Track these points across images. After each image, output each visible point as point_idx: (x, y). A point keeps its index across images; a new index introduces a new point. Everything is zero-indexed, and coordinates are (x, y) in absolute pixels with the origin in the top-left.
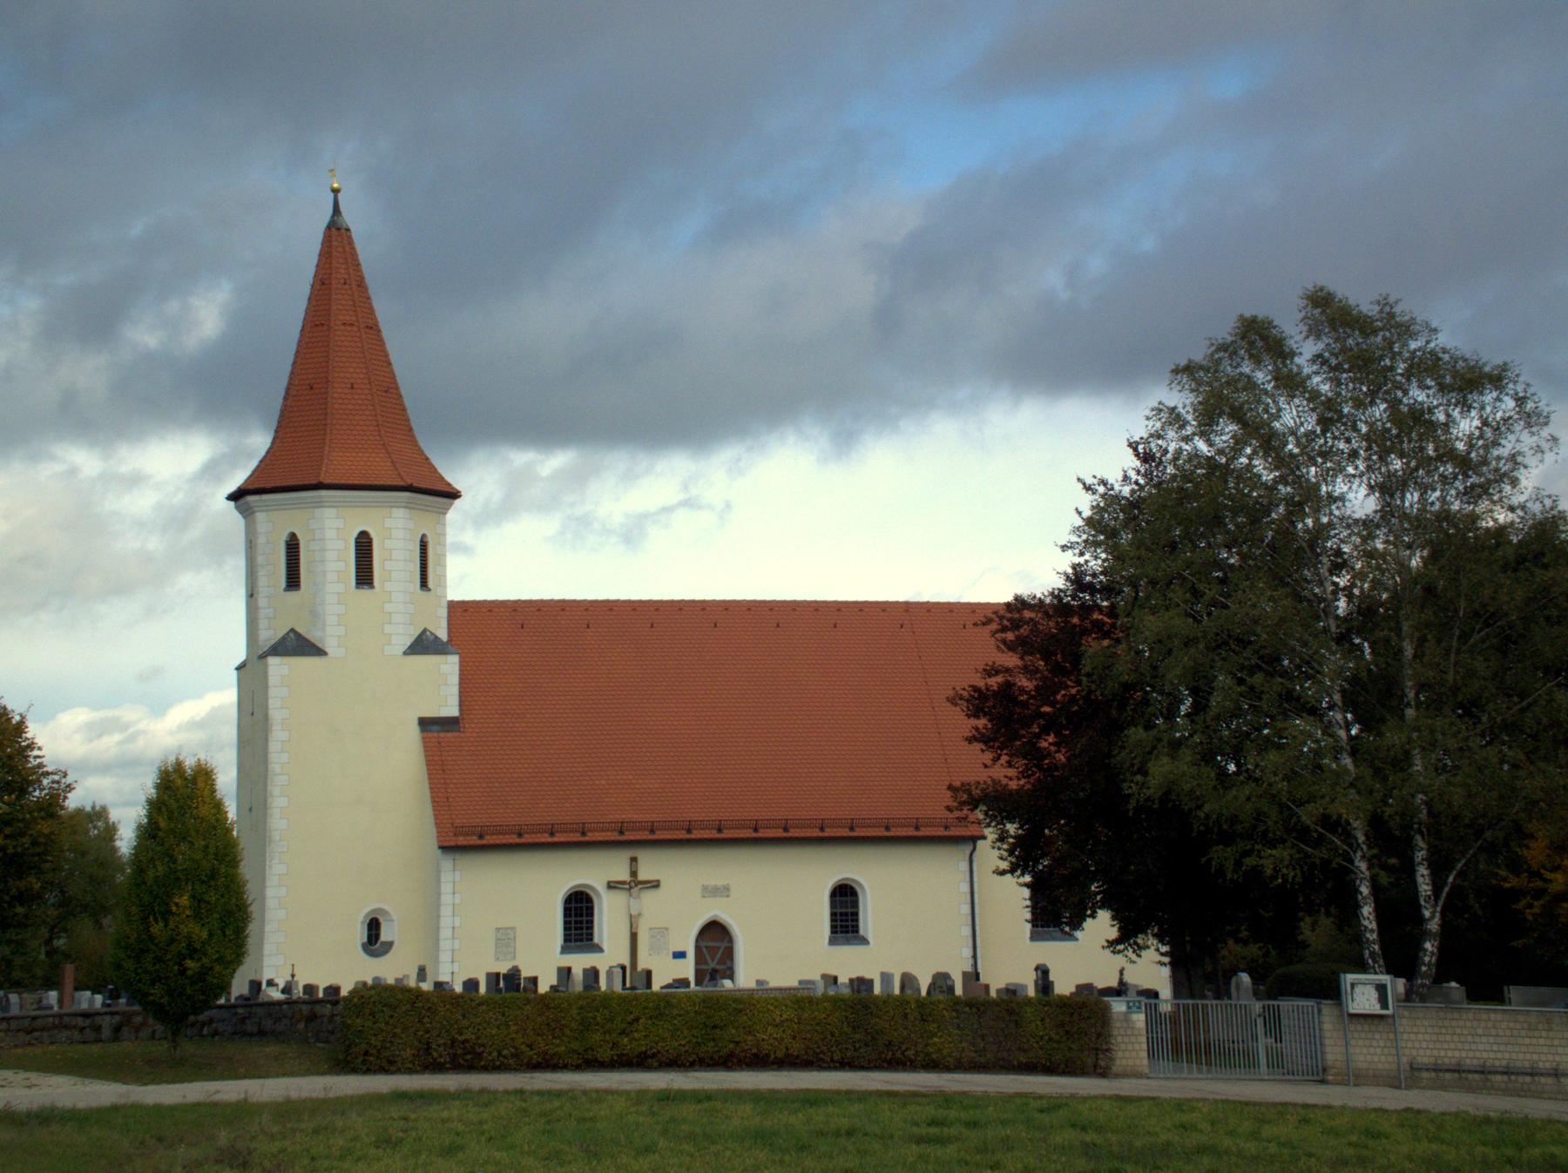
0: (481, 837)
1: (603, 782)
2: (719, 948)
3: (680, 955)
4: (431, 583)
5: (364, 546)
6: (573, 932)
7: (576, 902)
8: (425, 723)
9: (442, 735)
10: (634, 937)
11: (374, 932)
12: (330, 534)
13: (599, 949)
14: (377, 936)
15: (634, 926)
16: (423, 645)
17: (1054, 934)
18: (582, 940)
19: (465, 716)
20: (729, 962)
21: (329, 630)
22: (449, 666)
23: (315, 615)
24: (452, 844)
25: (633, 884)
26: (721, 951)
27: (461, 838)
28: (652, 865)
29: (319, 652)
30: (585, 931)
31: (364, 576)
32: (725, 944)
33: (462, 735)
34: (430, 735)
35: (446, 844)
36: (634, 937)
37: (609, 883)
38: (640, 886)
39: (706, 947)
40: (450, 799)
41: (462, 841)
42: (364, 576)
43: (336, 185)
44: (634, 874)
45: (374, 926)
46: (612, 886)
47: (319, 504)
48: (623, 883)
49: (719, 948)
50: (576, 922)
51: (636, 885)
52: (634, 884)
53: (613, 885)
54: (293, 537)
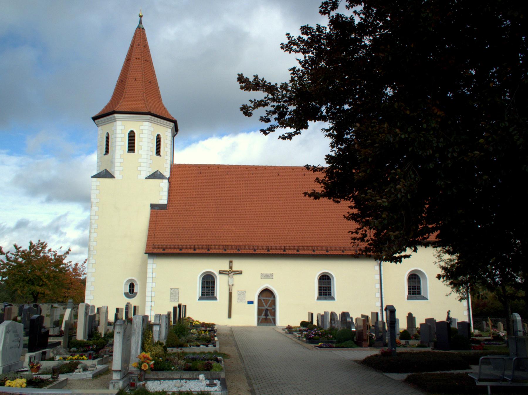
2: (269, 300)
3: (251, 302)
4: (162, 154)
5: (132, 136)
8: (153, 206)
9: (159, 211)
10: (230, 294)
11: (132, 288)
12: (118, 131)
14: (133, 290)
15: (230, 290)
16: (156, 176)
17: (418, 297)
19: (170, 204)
21: (116, 169)
22: (164, 184)
23: (112, 163)
25: (230, 272)
26: (270, 301)
27: (155, 250)
28: (238, 264)
29: (112, 177)
30: (210, 291)
31: (131, 148)
32: (272, 299)
33: (167, 211)
34: (154, 210)
36: (230, 294)
37: (220, 271)
39: (264, 300)
40: (156, 235)
41: (155, 251)
42: (131, 148)
43: (141, 14)
44: (231, 268)
45: (132, 286)
46: (221, 273)
47: (115, 120)
48: (226, 271)
49: (269, 300)
50: (207, 287)
51: (232, 273)
52: (231, 272)
53: (221, 272)
54: (108, 133)
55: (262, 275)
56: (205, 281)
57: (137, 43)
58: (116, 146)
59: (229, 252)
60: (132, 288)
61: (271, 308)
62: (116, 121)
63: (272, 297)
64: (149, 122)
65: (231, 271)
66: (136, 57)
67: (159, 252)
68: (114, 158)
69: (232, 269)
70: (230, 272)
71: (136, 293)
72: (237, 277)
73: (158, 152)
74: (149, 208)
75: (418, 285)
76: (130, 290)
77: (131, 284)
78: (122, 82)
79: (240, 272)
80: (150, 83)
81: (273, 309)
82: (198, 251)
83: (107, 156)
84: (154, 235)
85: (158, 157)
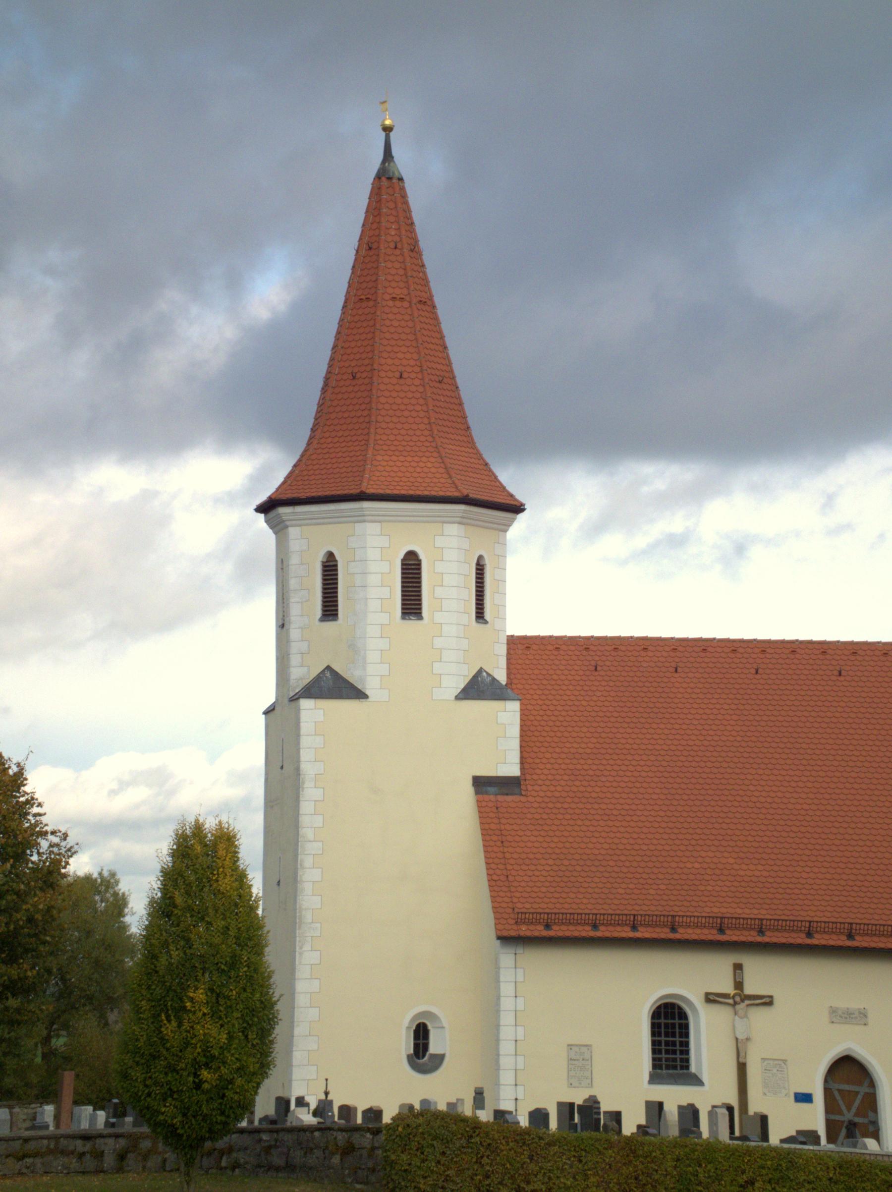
0: (548, 926)
6: (664, 1056)
10: (742, 1069)
11: (421, 1041)
13: (696, 1081)
14: (426, 1047)
15: (742, 1054)
18: (675, 1068)
21: (370, 669)
23: (354, 649)
29: (358, 694)
30: (678, 1056)
36: (742, 1069)
38: (747, 1002)
40: (510, 878)
44: (739, 985)
45: (421, 1034)
46: (711, 999)
50: (667, 1043)
51: (742, 1001)
53: (711, 997)
54: (330, 556)
76: (416, 1046)
77: (419, 1026)
78: (354, 378)
79: (767, 1000)
83: (330, 625)
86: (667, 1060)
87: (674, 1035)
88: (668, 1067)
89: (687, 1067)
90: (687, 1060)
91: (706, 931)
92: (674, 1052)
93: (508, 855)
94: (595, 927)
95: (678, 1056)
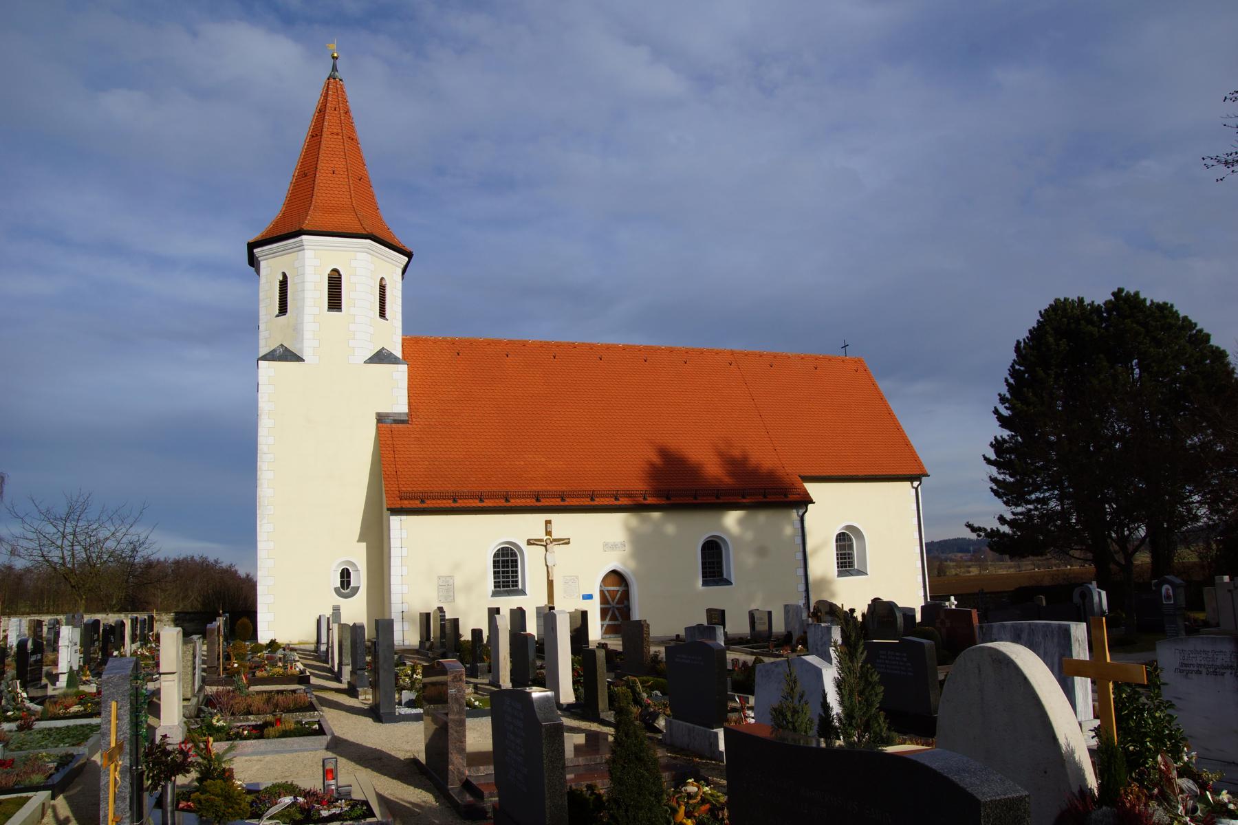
0: (422, 501)
1: (522, 463)
3: (589, 597)
5: (335, 282)
6: (501, 580)
7: (503, 556)
8: (381, 418)
9: (394, 425)
10: (550, 584)
11: (345, 579)
12: (309, 270)
13: (523, 592)
14: (349, 583)
15: (551, 575)
16: (382, 357)
20: (626, 602)
21: (307, 343)
22: (399, 374)
23: (297, 330)
24: (399, 506)
25: (548, 542)
26: (620, 593)
27: (406, 502)
28: (563, 523)
29: (300, 359)
30: (511, 579)
31: (335, 302)
33: (409, 426)
34: (385, 425)
35: (393, 506)
36: (550, 584)
39: (607, 591)
41: (406, 504)
42: (335, 302)
43: (336, 55)
44: (548, 533)
45: (345, 574)
46: (530, 543)
47: (301, 247)
48: (541, 540)
50: (503, 572)
51: (551, 542)
52: (547, 542)
53: (532, 542)
54: (284, 275)
55: (606, 545)
56: (498, 561)
57: (332, 106)
58: (304, 298)
59: (547, 504)
60: (345, 579)
61: (623, 606)
62: (304, 250)
63: (623, 585)
64: (366, 252)
65: (549, 539)
66: (330, 130)
67: (414, 506)
68: (302, 323)
69: (551, 536)
70: (548, 542)
71: (356, 589)
72: (557, 549)
73: (382, 314)
74: (373, 422)
75: (850, 552)
76: (342, 583)
77: (343, 569)
78: (306, 176)
80: (360, 180)
81: (625, 607)
82: (488, 503)
84: (395, 473)
85: (382, 320)
86: (503, 582)
87: (508, 567)
88: (504, 587)
89: (517, 586)
90: (517, 581)
91: (528, 500)
92: (508, 577)
93: (397, 459)
94: (455, 500)
95: (511, 579)
